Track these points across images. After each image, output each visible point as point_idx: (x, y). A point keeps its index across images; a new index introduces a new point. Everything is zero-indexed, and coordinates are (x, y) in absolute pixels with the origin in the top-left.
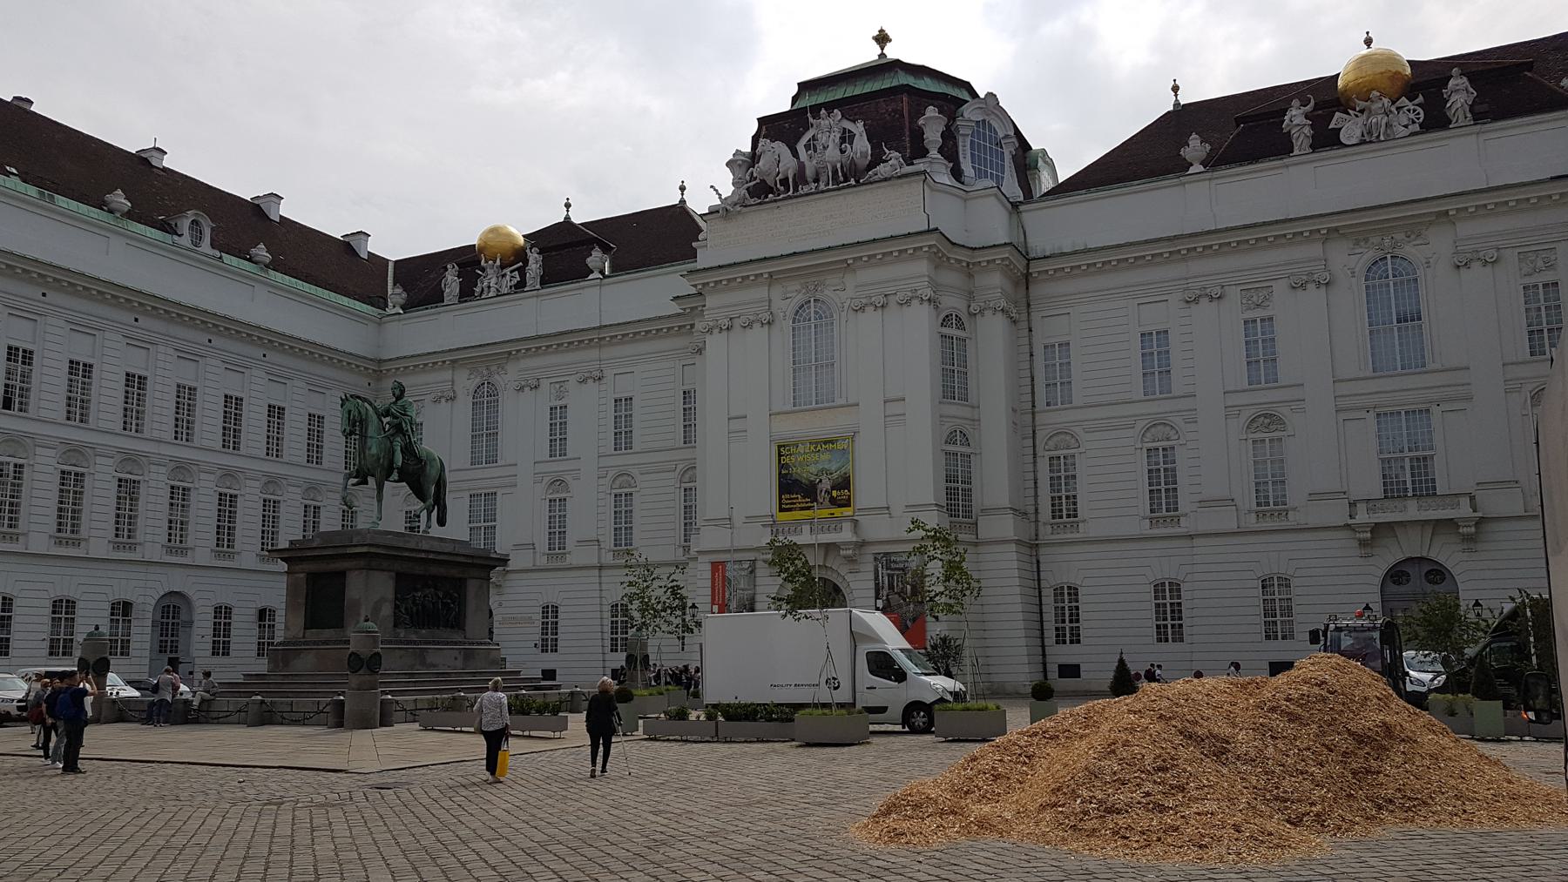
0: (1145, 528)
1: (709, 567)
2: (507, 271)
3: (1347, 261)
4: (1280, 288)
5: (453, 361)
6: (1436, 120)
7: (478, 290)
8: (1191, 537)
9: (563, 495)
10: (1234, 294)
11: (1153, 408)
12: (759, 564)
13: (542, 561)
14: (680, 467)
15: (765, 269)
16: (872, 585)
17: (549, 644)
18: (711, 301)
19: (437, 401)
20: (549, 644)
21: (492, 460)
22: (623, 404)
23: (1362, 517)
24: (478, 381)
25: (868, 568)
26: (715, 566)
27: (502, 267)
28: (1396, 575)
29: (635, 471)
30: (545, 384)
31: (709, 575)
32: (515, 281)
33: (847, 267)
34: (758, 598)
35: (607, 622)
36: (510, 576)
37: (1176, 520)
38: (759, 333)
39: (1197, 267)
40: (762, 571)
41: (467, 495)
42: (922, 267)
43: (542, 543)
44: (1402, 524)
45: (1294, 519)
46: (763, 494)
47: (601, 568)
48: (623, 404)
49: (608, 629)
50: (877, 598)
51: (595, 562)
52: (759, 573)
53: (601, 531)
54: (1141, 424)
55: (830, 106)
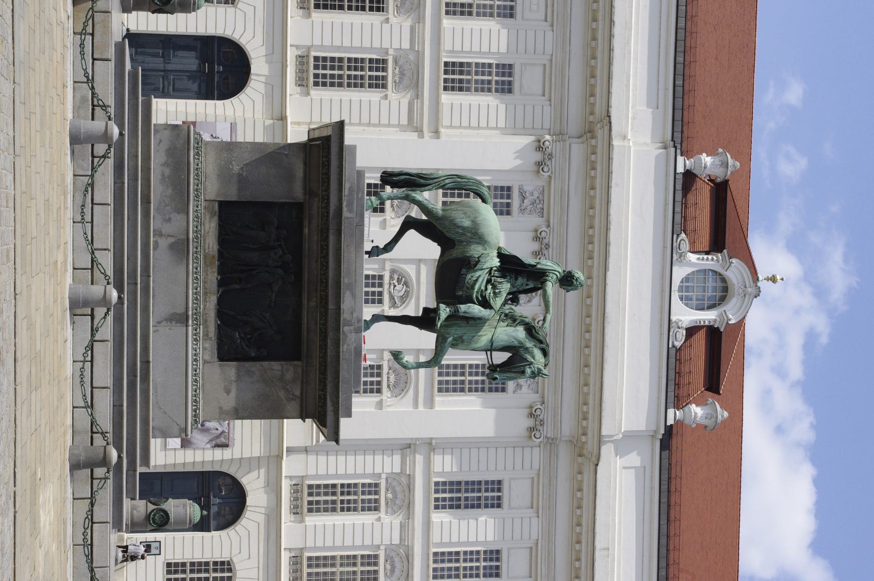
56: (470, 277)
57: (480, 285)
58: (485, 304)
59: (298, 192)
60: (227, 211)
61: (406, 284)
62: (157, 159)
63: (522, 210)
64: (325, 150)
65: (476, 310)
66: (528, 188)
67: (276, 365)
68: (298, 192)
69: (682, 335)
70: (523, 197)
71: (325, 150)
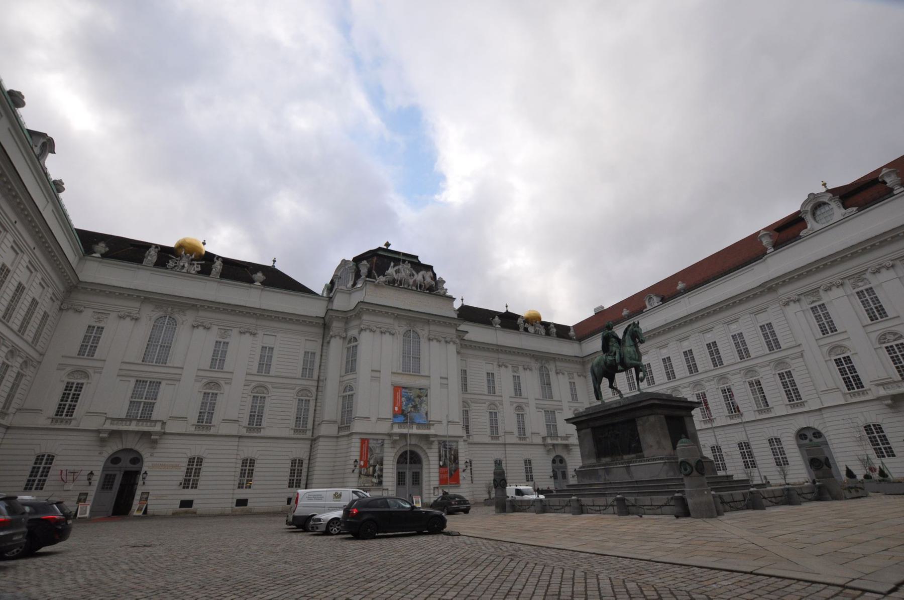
0: (487, 440)
1: (359, 441)
2: (195, 263)
3: (535, 365)
4: (521, 368)
5: (145, 298)
6: (548, 334)
7: (171, 264)
8: (505, 444)
9: (215, 392)
10: (510, 366)
11: (490, 398)
12: (386, 442)
13: (192, 430)
14: (297, 388)
15: (397, 312)
16: (437, 454)
17: (190, 481)
18: (365, 317)
19: (121, 317)
20: (190, 481)
21: (163, 361)
22: (267, 352)
23: (549, 441)
24: (161, 314)
25: (435, 446)
26: (363, 441)
27: (192, 260)
28: (554, 461)
29: (269, 386)
30: (215, 329)
31: (358, 445)
32: (199, 269)
33: (428, 322)
34: (385, 458)
35: (239, 470)
36: (166, 437)
37: (498, 438)
38: (387, 337)
39: (501, 356)
40: (387, 445)
41: (133, 381)
42: (454, 331)
43: (194, 418)
44: (557, 445)
45: (528, 441)
46: (387, 409)
47: (240, 437)
48: (267, 352)
49: (238, 474)
50: (440, 460)
51: (235, 433)
52: (386, 446)
53: (241, 416)
54: (488, 403)
55: (409, 262)
56: (608, 362)
57: (610, 358)
58: (615, 354)
59: (589, 430)
60: (599, 454)
61: (884, 335)
62: (586, 481)
63: (820, 300)
64: (580, 421)
65: (617, 357)
66: (809, 301)
67: (639, 428)
68: (589, 430)
69: (849, 210)
70: (814, 302)
71: (580, 421)
